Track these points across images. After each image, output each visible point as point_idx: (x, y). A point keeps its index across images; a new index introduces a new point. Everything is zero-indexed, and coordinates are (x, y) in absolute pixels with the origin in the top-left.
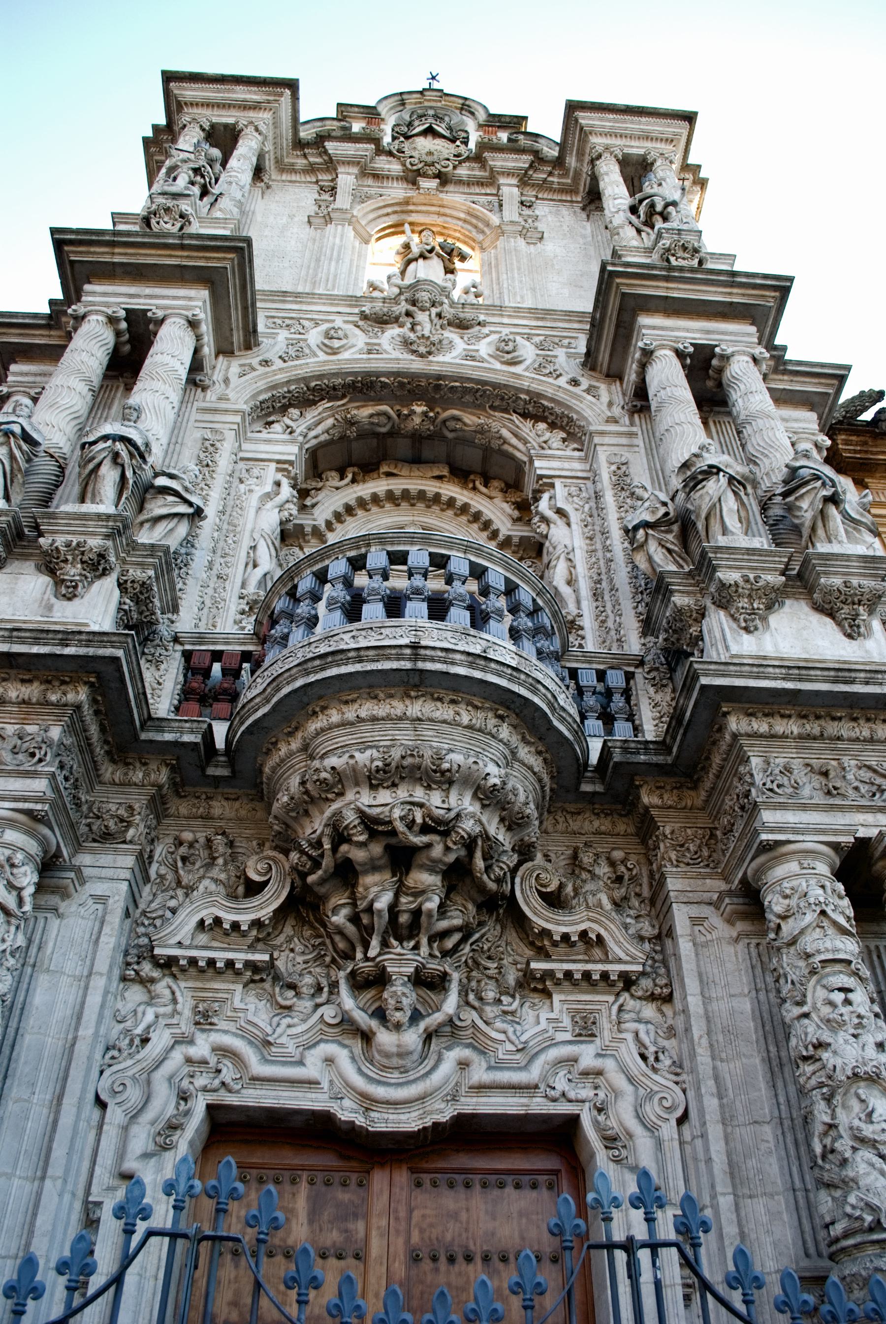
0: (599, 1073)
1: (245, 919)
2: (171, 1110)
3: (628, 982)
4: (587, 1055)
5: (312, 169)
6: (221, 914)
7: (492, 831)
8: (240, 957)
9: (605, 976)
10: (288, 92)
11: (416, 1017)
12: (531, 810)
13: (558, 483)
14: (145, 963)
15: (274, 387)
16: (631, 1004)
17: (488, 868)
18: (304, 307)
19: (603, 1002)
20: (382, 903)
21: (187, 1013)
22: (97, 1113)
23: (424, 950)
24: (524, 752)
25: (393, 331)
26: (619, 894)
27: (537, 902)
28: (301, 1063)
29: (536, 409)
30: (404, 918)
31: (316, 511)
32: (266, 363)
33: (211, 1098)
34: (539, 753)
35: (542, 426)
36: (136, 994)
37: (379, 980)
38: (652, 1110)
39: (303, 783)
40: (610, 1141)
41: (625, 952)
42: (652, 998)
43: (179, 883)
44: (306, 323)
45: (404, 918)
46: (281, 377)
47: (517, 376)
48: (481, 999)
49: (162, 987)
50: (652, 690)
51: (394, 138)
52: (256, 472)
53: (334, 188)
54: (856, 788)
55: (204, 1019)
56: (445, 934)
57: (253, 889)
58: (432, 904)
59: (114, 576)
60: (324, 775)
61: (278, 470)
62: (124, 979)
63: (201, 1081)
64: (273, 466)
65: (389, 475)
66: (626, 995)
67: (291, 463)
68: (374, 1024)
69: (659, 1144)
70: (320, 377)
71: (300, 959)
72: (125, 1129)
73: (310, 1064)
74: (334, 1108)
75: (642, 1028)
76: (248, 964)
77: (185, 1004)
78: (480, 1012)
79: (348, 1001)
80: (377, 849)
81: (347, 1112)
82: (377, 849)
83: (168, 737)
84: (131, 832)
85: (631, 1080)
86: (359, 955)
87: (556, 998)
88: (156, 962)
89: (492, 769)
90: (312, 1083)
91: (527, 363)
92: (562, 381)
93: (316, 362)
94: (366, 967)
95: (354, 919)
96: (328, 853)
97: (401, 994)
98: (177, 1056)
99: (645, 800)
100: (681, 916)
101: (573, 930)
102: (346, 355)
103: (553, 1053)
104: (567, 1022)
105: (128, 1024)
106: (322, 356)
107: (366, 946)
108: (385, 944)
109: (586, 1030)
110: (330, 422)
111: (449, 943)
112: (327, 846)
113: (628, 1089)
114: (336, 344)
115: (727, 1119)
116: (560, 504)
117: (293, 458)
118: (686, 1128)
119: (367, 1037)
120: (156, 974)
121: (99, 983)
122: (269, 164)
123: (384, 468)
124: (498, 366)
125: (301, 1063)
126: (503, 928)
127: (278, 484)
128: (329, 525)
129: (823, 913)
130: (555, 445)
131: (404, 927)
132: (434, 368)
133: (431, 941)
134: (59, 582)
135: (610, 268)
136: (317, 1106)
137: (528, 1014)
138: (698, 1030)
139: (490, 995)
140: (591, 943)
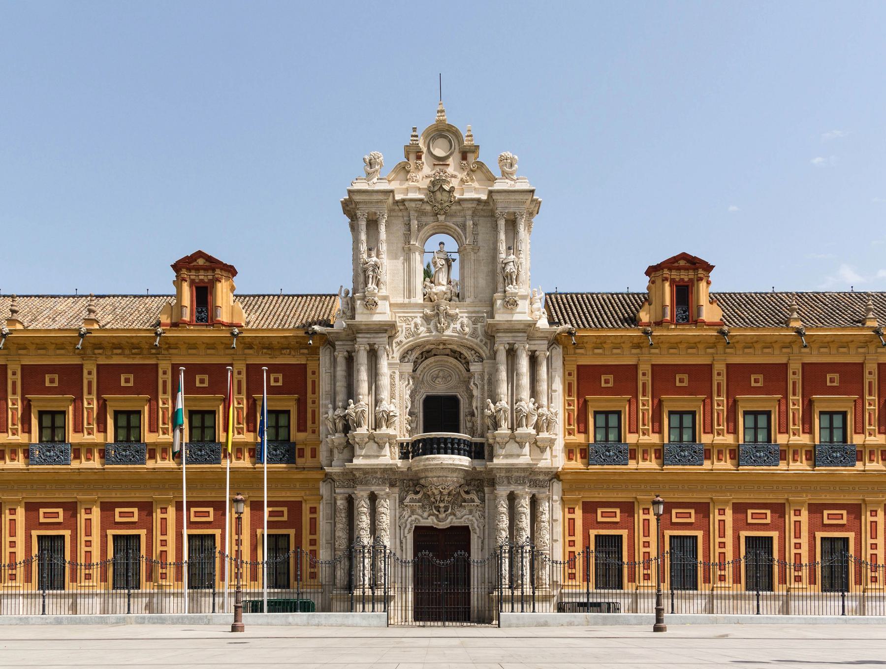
4: (470, 517)
35: (473, 352)
57: (417, 493)
73: (431, 521)
97: (442, 510)
109: (471, 512)
131: (442, 501)
138: (486, 515)
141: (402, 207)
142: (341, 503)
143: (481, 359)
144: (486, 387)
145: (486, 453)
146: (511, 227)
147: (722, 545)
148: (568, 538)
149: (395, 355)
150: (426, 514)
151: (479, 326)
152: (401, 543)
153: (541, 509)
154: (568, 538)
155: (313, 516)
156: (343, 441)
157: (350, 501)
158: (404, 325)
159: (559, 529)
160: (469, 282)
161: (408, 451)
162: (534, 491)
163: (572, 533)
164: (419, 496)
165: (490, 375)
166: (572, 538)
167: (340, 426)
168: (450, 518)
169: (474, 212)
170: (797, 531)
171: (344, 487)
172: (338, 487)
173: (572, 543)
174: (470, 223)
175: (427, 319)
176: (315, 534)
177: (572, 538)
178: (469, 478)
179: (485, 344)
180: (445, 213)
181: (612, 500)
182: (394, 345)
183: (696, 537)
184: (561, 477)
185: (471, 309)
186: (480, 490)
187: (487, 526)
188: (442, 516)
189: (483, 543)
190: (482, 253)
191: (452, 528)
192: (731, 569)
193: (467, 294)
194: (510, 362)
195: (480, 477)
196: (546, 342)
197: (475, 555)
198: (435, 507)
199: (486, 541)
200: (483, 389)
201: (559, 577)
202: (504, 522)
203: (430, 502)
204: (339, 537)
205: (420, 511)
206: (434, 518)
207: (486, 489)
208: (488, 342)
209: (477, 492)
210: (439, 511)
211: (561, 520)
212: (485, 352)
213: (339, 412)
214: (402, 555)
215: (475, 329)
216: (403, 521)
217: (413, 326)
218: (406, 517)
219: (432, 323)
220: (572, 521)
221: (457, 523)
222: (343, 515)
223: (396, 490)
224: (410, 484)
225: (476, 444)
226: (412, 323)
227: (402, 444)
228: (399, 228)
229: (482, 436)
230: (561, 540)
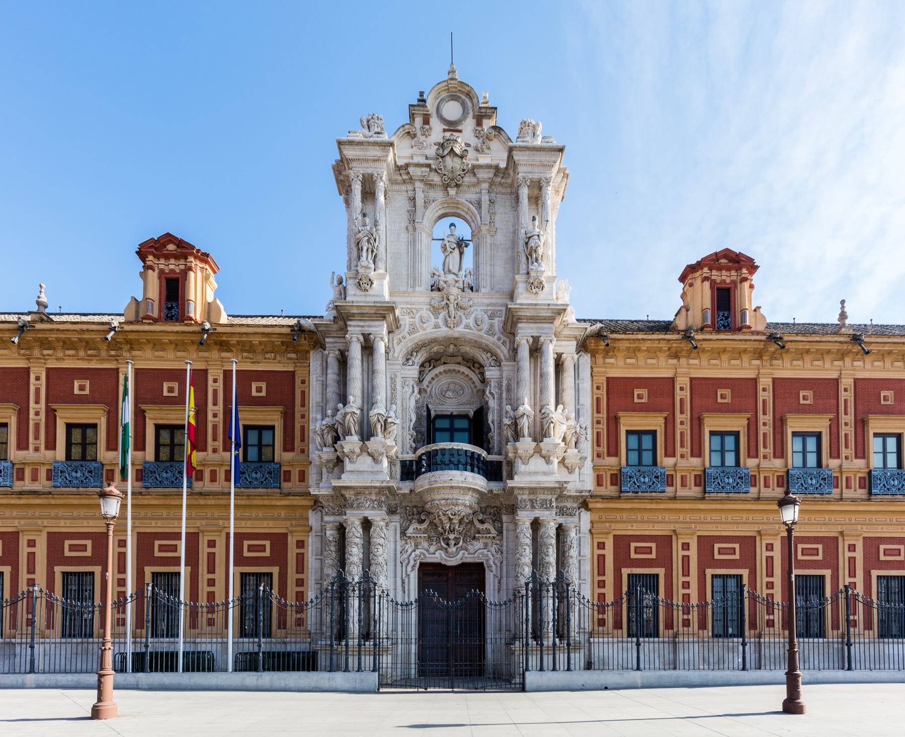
4: (485, 551)
5: (404, 182)
14: (403, 533)
18: (414, 300)
19: (489, 541)
25: (443, 313)
32: (404, 338)
36: (403, 542)
37: (448, 539)
38: (496, 561)
41: (494, 533)
44: (414, 311)
47: (481, 337)
49: (408, 541)
55: (416, 546)
57: (421, 522)
73: (437, 556)
93: (419, 336)
97: (453, 542)
100: (505, 525)
102: (428, 330)
106: (421, 332)
109: (486, 546)
115: (507, 565)
121: (399, 544)
124: (476, 332)
132: (456, 335)
137: (475, 543)
138: (505, 548)
141: (405, 177)
142: (331, 534)
143: (498, 363)
144: (504, 395)
145: (504, 474)
146: (534, 206)
147: (770, 585)
148: (597, 578)
150: (432, 549)
152: (403, 583)
153: (569, 543)
154: (597, 578)
155: (300, 551)
156: (333, 457)
157: (342, 530)
158: (407, 317)
159: (587, 567)
160: (485, 269)
161: (409, 471)
162: (561, 520)
163: (601, 571)
164: (425, 526)
165: (509, 380)
166: (602, 578)
167: (329, 439)
168: (461, 552)
169: (491, 185)
170: (852, 569)
171: (334, 514)
172: (327, 514)
173: (602, 584)
174: (485, 198)
175: (435, 310)
176: (303, 573)
177: (602, 578)
178: (484, 505)
179: (504, 343)
180: (457, 186)
181: (647, 533)
182: (395, 342)
183: (741, 576)
184: (591, 506)
185: (486, 301)
186: (496, 518)
187: (505, 562)
188: (453, 549)
189: (499, 583)
191: (464, 566)
192: (696, 613)
193: (482, 283)
194: (532, 365)
195: (497, 503)
196: (575, 343)
197: (491, 594)
198: (444, 540)
199: (504, 580)
200: (500, 398)
201: (587, 625)
202: (527, 557)
203: (438, 534)
204: (328, 575)
205: (426, 544)
206: (443, 553)
208: (508, 340)
209: (494, 521)
210: (448, 544)
211: (589, 556)
212: (503, 352)
213: (327, 421)
214: (404, 598)
215: (492, 326)
216: (405, 556)
217: (417, 320)
218: (410, 551)
219: (441, 316)
220: (601, 559)
221: (469, 559)
222: (333, 549)
223: (397, 518)
224: (416, 512)
225: (492, 462)
226: (417, 316)
227: (403, 463)
228: (401, 202)
229: (500, 454)
230: (589, 581)
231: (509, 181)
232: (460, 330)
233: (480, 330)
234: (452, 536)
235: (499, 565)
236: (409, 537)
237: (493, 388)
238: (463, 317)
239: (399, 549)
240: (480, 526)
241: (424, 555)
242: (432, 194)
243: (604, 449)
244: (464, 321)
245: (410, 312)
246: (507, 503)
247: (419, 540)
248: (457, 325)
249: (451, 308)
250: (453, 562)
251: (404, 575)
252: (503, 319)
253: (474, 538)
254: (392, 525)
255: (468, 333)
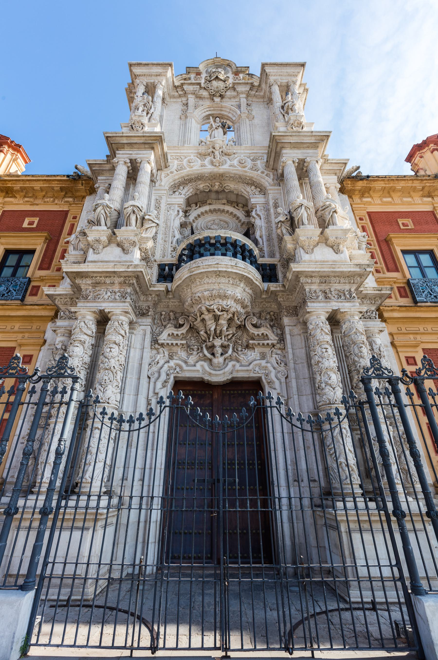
0: (266, 367)
1: (179, 333)
2: (165, 378)
3: (273, 346)
4: (263, 363)
5: (180, 96)
6: (174, 332)
7: (239, 310)
8: (179, 342)
9: (268, 344)
10: (170, 68)
11: (222, 354)
12: (249, 304)
13: (258, 206)
15: (175, 180)
16: (274, 350)
17: (238, 319)
18: (182, 151)
19: (267, 350)
20: (213, 329)
21: (167, 356)
22: (148, 379)
23: (223, 339)
24: (247, 289)
25: (208, 159)
26: (272, 324)
27: (251, 326)
28: (195, 366)
29: (252, 183)
30: (218, 332)
31: (190, 217)
32: (172, 172)
33: (175, 375)
34: (251, 289)
35: (253, 187)
36: (154, 352)
37: (213, 346)
38: (279, 375)
39: (191, 300)
40: (268, 383)
41: (273, 338)
42: (280, 349)
43: (162, 325)
44: (183, 157)
45: (218, 332)
46: (177, 177)
47: (246, 172)
48: (237, 350)
49: (161, 350)
50: (282, 269)
51: (205, 82)
52: (172, 208)
53: (187, 104)
54: (334, 297)
55: (171, 357)
56: (228, 335)
57: (181, 326)
58: (225, 329)
59: (137, 247)
60: (196, 298)
61: (178, 207)
62: (151, 348)
63: (171, 371)
64: (177, 206)
65: (210, 204)
66: (273, 348)
67: (182, 204)
68: (212, 357)
69: (281, 383)
70: (188, 176)
71: (193, 342)
72: (155, 383)
74: (203, 376)
75: (277, 356)
76: (181, 344)
77: (166, 353)
78: (237, 353)
79: (206, 352)
80: (211, 315)
81: (207, 378)
82: (211, 315)
83: (156, 289)
84: (150, 313)
85: (274, 368)
86: (208, 341)
87: (256, 349)
88: (159, 344)
89: (239, 295)
90: (198, 371)
91: (249, 166)
92: (259, 172)
93: (186, 171)
94: (209, 344)
95: (206, 332)
96: (199, 317)
98: (166, 365)
99: (279, 300)
100: (287, 329)
101: (260, 333)
102: (194, 168)
103: (255, 363)
104: (258, 355)
105: (153, 359)
107: (209, 339)
108: (213, 338)
109: (263, 356)
110: (192, 190)
111: (229, 337)
112: (198, 315)
113: (274, 371)
114: (192, 164)
115: (297, 378)
116: (258, 213)
117: (182, 203)
118: (287, 380)
119: (210, 360)
120: (159, 347)
122: (167, 96)
123: (208, 202)
124: (240, 168)
125: (195, 366)
126: (243, 332)
127: (178, 211)
128: (193, 221)
129: (322, 329)
130: (257, 194)
131: (218, 335)
133: (225, 337)
134: (124, 250)
135: (273, 134)
136: (200, 376)
138: (291, 356)
139: (240, 349)
140: (265, 337)
141: (180, 93)
143: (263, 191)
145: (280, 276)
149: (163, 183)
151: (259, 162)
164: (183, 330)
168: (231, 364)
175: (202, 156)
187: (292, 375)
188: (219, 360)
190: (256, 121)
205: (183, 354)
206: (206, 365)
207: (286, 321)
210: (213, 354)
212: (267, 181)
216: (155, 368)
218: (162, 362)
223: (148, 321)
226: (185, 160)
231: (262, 94)
232: (225, 168)
233: (245, 167)
234: (218, 342)
235: (283, 380)
236: (162, 345)
237: (259, 210)
238: (228, 160)
239: (146, 360)
240: (255, 331)
241: (181, 367)
242: (201, 102)
243: (382, 265)
244: (229, 162)
245: (179, 158)
246: (287, 304)
247: (175, 349)
248: (221, 164)
249: (217, 153)
250: (219, 377)
251: (151, 394)
252: (265, 160)
253: (247, 347)
254: (139, 330)
255: (233, 170)
